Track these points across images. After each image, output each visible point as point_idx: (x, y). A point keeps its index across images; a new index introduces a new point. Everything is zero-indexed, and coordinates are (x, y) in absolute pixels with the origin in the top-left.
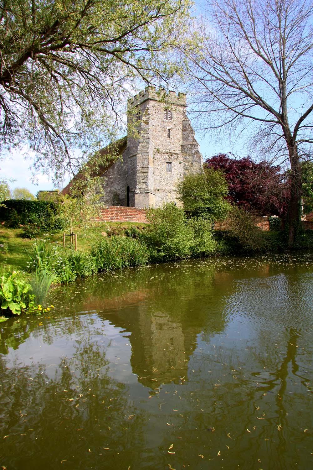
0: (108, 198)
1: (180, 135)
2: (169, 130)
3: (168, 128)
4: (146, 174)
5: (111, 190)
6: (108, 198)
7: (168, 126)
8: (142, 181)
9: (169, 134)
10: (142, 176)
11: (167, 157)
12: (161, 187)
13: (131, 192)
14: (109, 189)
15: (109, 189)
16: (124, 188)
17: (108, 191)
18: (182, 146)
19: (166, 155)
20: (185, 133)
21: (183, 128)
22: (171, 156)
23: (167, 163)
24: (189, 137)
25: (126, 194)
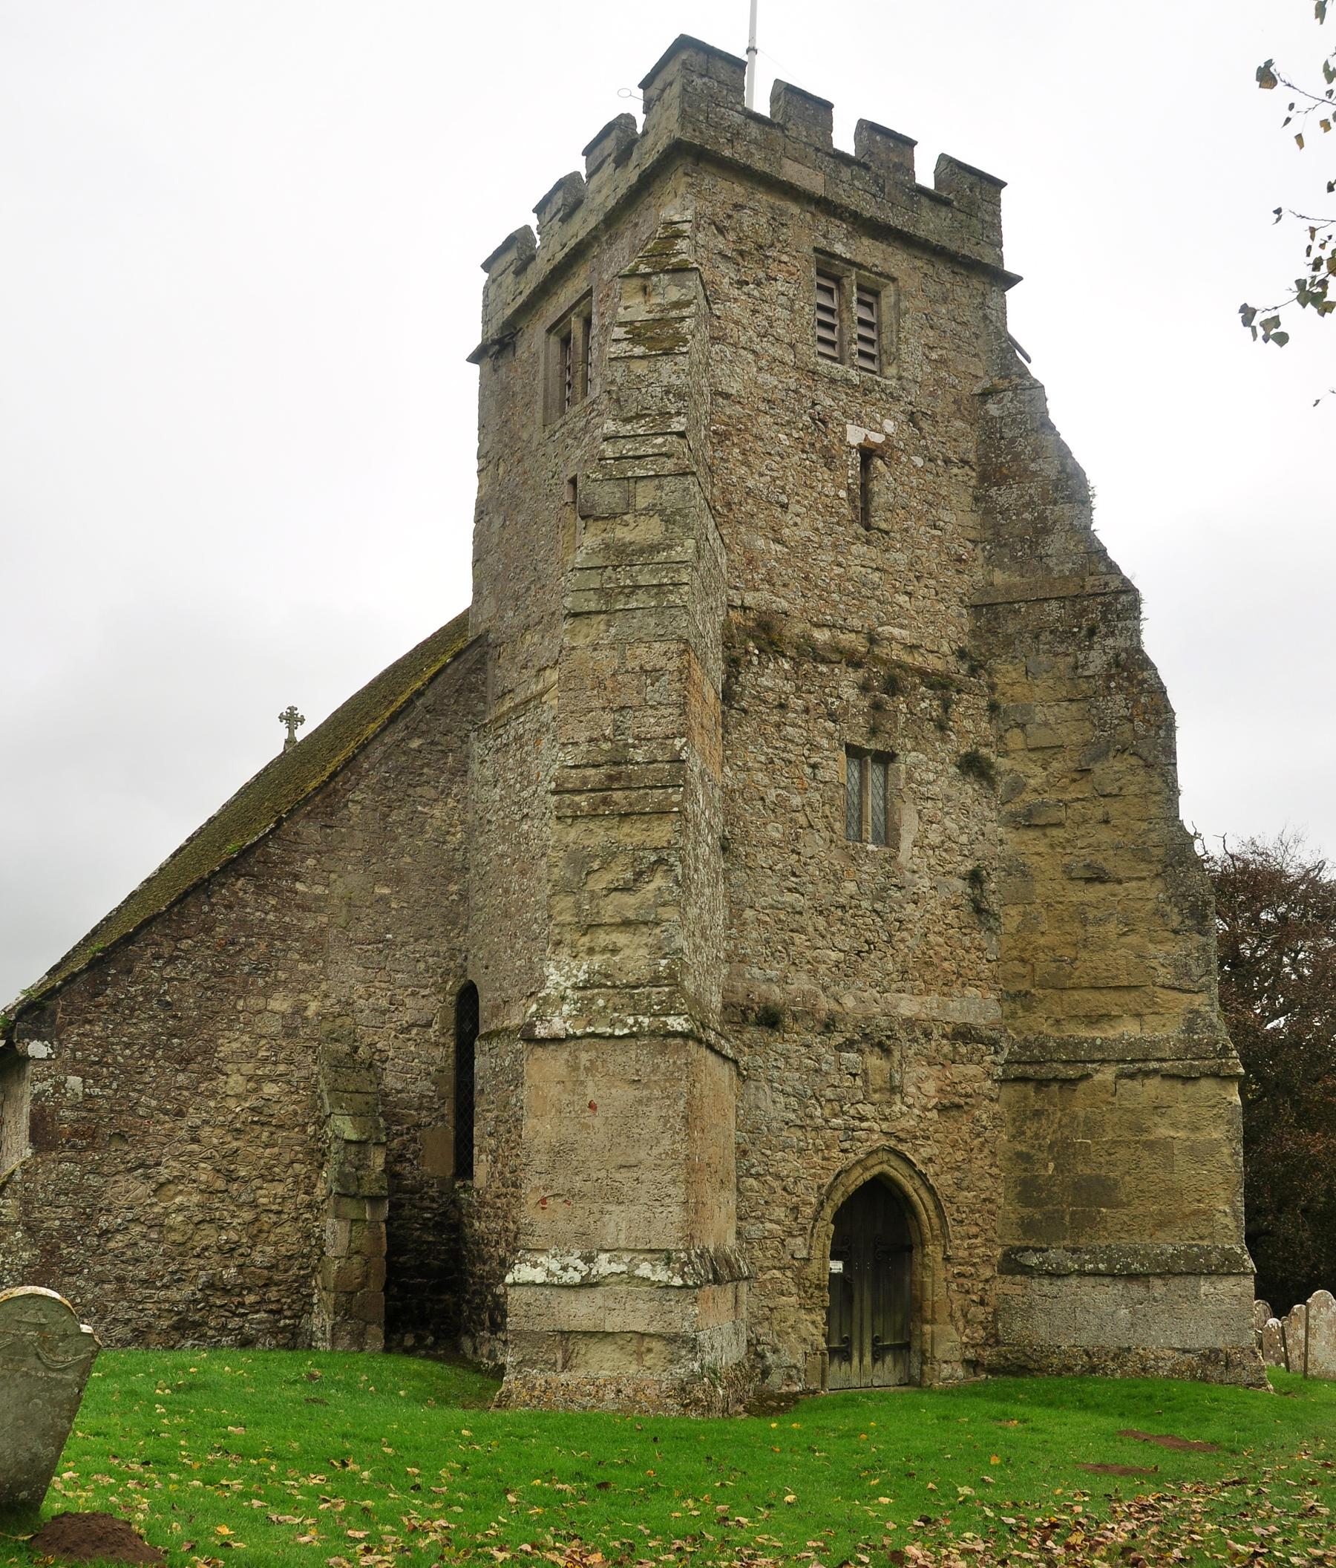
0: (270, 1089)
1: (958, 516)
2: (867, 453)
3: (855, 435)
4: (662, 832)
5: (299, 1010)
7: (859, 420)
8: (612, 908)
9: (864, 487)
10: (609, 856)
11: (850, 693)
12: (801, 982)
13: (489, 1036)
14: (280, 1003)
15: (280, 1003)
16: (433, 1006)
17: (275, 1026)
18: (986, 610)
19: (847, 685)
20: (1005, 496)
21: (983, 458)
22: (892, 687)
23: (854, 752)
24: (1042, 529)
25: (442, 1055)
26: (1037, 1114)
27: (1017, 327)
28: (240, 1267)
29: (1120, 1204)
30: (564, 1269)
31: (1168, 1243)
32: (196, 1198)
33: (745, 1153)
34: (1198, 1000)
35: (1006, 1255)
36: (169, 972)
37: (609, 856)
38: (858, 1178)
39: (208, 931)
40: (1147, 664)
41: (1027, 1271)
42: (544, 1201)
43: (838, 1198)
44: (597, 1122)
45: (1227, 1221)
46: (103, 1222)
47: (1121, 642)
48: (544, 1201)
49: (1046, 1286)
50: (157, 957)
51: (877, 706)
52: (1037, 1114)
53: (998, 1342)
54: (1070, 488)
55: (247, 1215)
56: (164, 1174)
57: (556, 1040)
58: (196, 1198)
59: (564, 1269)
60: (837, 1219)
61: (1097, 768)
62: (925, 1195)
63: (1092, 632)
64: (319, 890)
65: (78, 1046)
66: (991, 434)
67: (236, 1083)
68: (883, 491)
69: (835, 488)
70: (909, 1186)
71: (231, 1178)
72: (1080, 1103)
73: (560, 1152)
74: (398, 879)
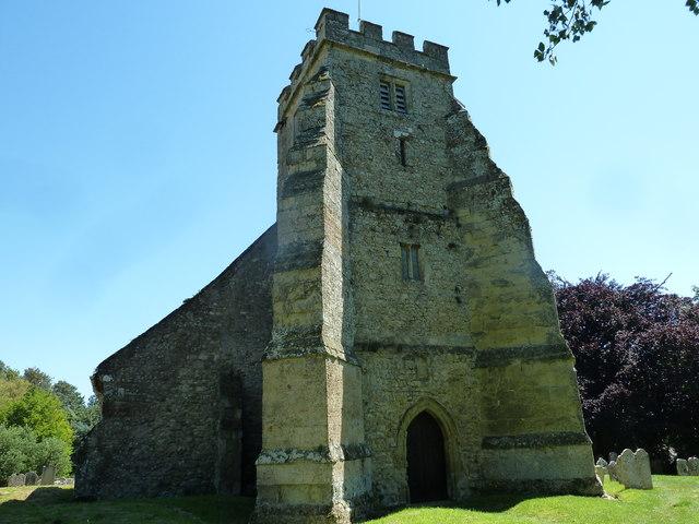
0: (199, 389)
1: (440, 158)
2: (402, 140)
5: (211, 359)
6: (199, 389)
7: (398, 128)
9: (402, 151)
12: (388, 333)
14: (203, 356)
15: (203, 356)
17: (201, 365)
18: (451, 188)
19: (399, 221)
20: (457, 151)
22: (417, 221)
26: (490, 381)
27: (457, 95)
28: (185, 460)
29: (526, 417)
30: (279, 457)
31: (554, 430)
32: (170, 433)
33: (366, 404)
34: (551, 329)
35: (484, 440)
36: (160, 347)
37: (296, 286)
38: (415, 412)
39: (175, 331)
40: (515, 203)
41: (492, 447)
42: (271, 427)
43: (409, 420)
44: (291, 393)
45: (577, 420)
46: (130, 445)
47: (505, 196)
48: (271, 427)
49: (502, 453)
50: (155, 342)
51: (411, 228)
52: (490, 381)
53: (485, 479)
54: (481, 142)
55: (189, 439)
56: (156, 424)
57: (274, 359)
58: (170, 433)
59: (279, 457)
60: (409, 430)
61: (500, 243)
62: (447, 418)
63: (493, 193)
64: (218, 314)
65: (124, 377)
66: (450, 129)
67: (184, 388)
68: (409, 152)
69: (391, 152)
70: (439, 414)
71: (183, 424)
72: (509, 374)
73: (277, 407)
74: (249, 308)
